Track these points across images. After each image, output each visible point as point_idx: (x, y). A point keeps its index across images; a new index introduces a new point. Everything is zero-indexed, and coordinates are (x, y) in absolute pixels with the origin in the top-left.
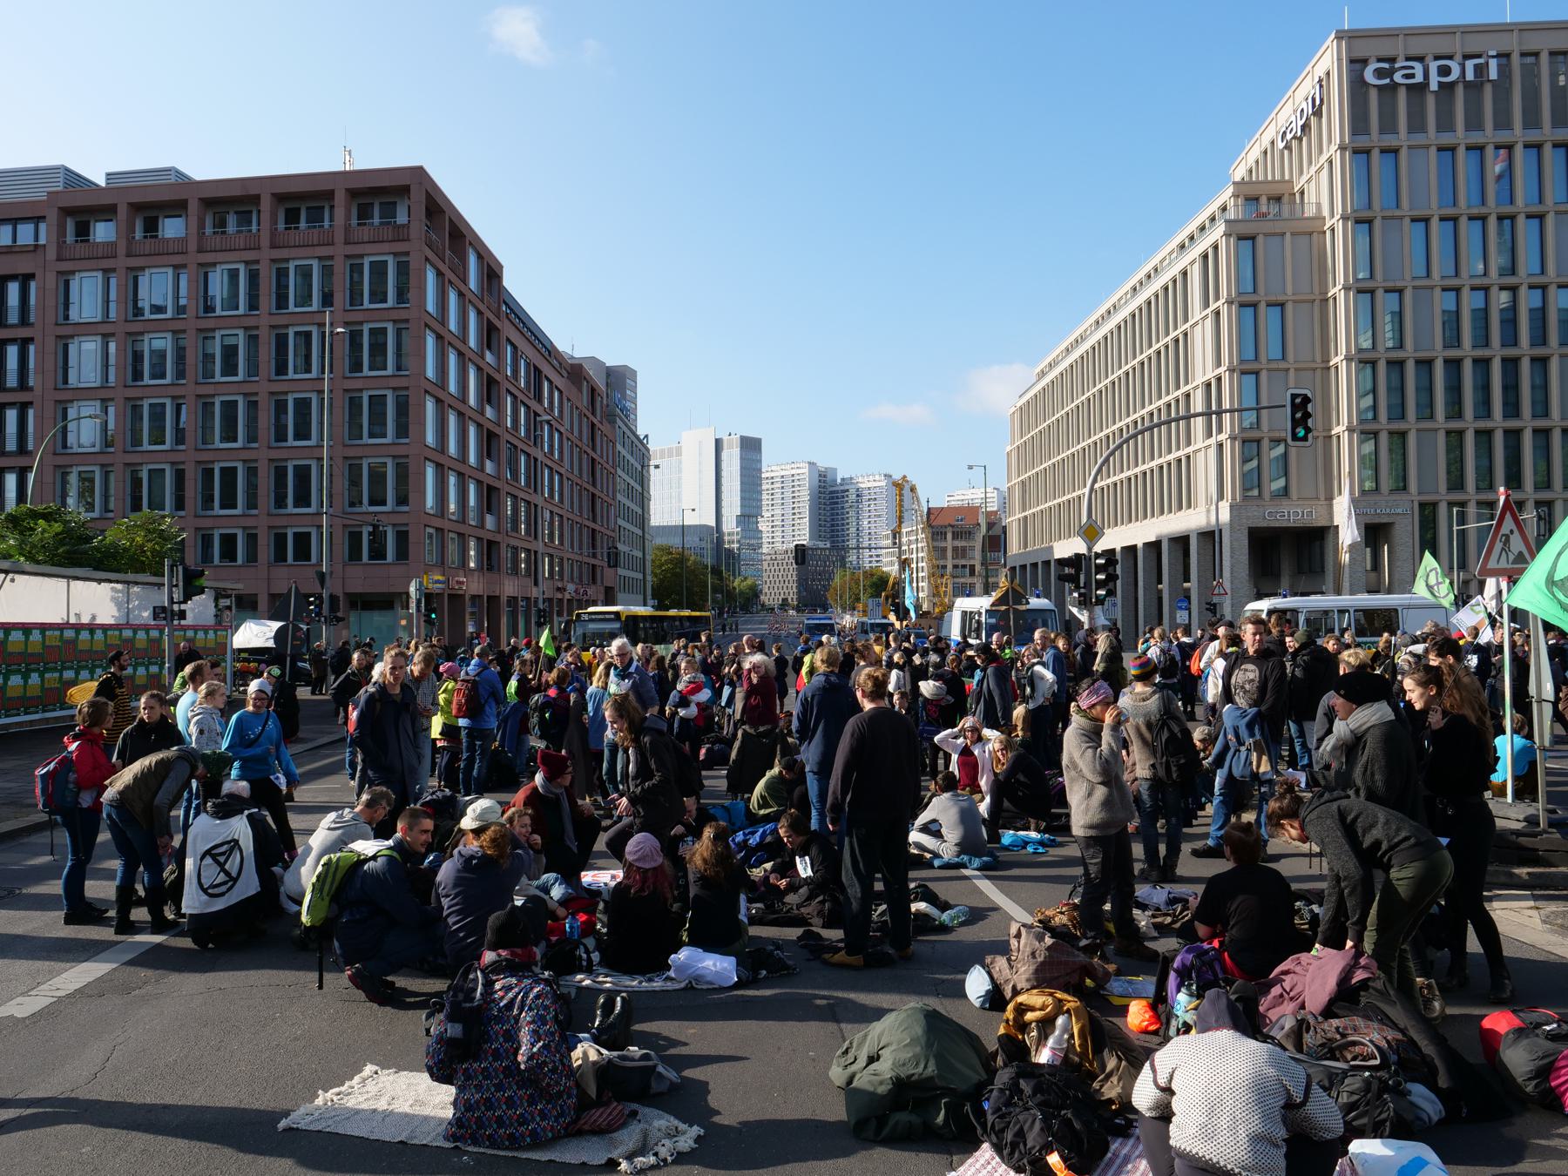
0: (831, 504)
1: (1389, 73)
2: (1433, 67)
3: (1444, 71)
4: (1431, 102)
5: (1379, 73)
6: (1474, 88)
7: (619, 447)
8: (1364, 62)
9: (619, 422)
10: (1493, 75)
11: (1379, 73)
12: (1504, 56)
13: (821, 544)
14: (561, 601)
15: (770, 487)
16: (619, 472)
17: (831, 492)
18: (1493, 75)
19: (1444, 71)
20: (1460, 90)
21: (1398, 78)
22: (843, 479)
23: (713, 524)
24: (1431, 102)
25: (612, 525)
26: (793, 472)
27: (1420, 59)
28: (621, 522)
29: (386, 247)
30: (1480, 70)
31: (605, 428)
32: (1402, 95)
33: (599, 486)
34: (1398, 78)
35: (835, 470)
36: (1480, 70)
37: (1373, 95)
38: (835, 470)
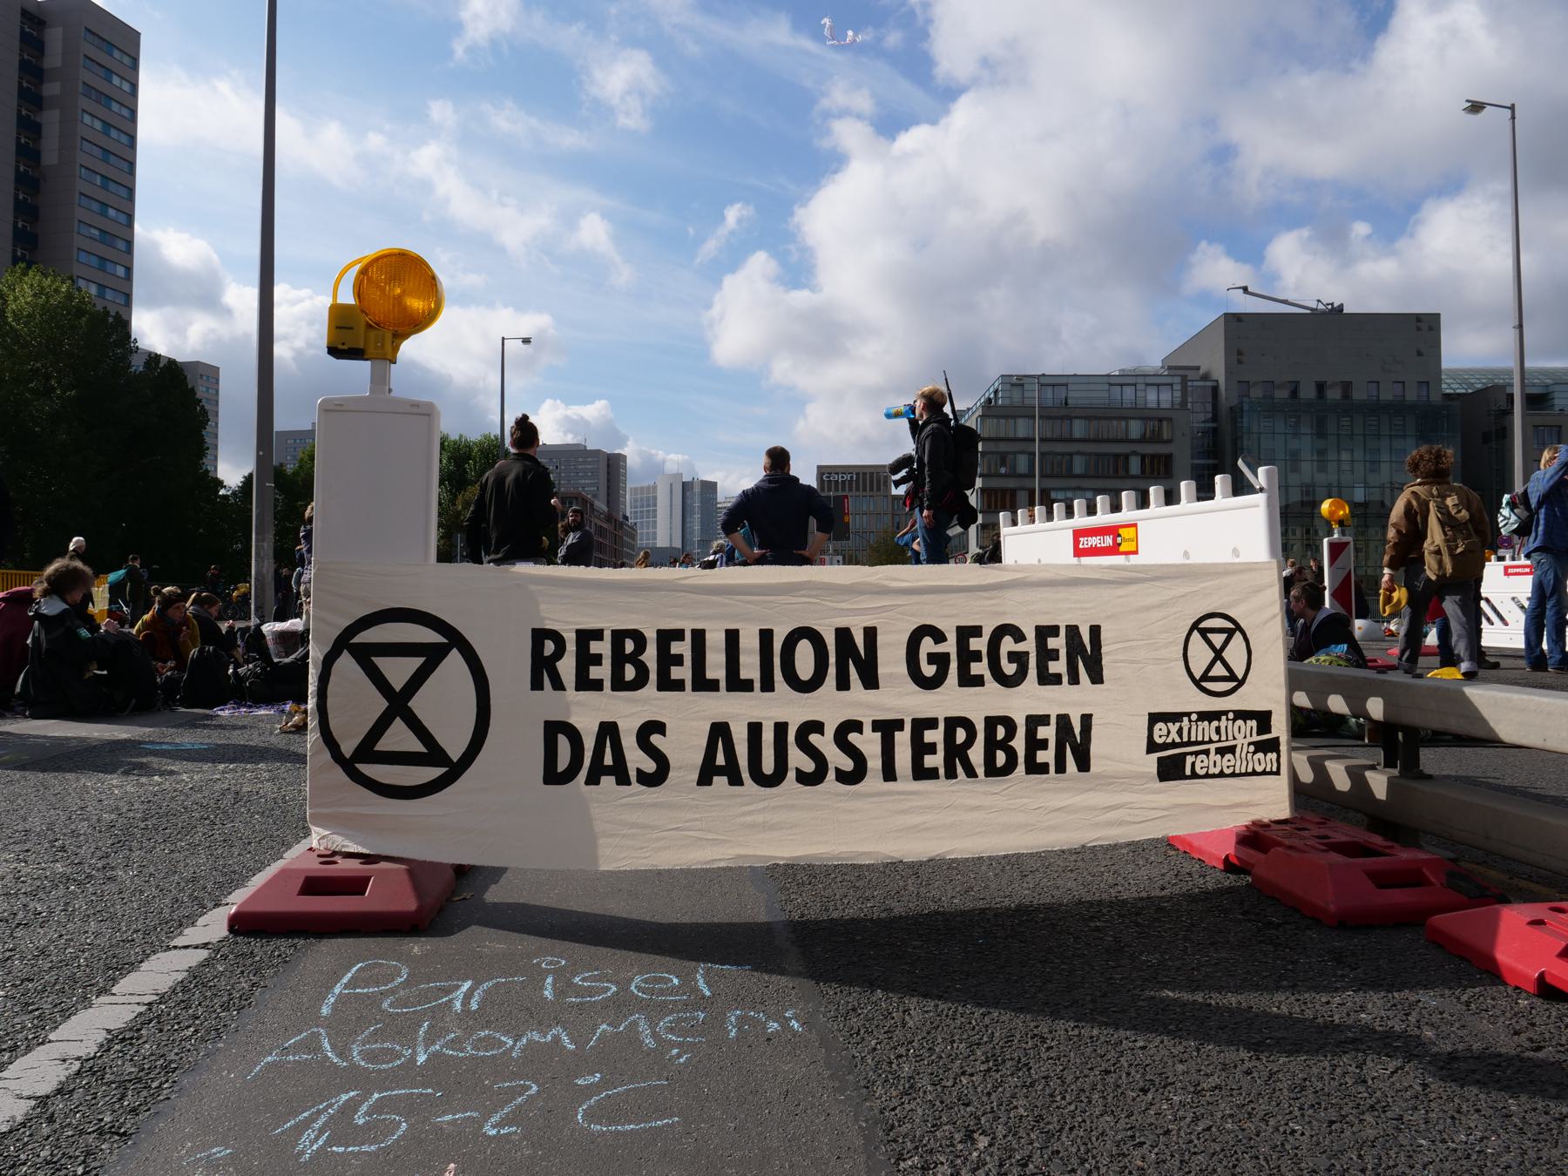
1: (829, 477)
2: (840, 476)
3: (843, 477)
4: (840, 485)
5: (827, 477)
6: (851, 481)
7: (625, 538)
8: (824, 474)
10: (854, 478)
11: (827, 477)
12: (857, 474)
16: (625, 549)
18: (854, 478)
19: (843, 477)
20: (847, 482)
21: (831, 478)
23: (680, 546)
24: (840, 485)
27: (837, 474)
30: (852, 477)
31: (620, 533)
32: (833, 483)
34: (831, 478)
36: (852, 477)
37: (826, 483)
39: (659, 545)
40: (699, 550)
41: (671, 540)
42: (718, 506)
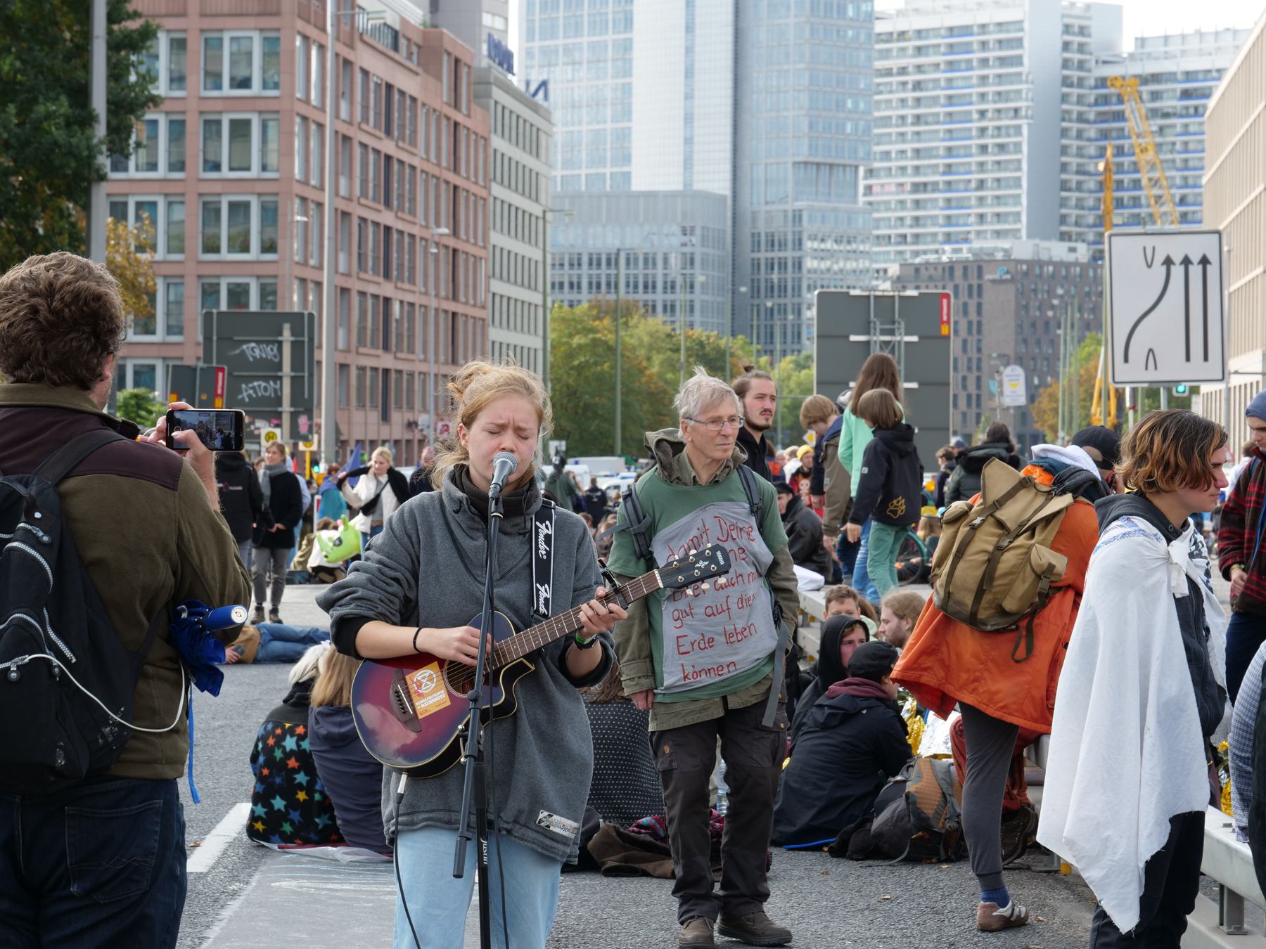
0: (1102, 118)
7: (497, 142)
9: (497, 94)
13: (1058, 251)
14: (409, 442)
15: (910, 62)
16: (497, 190)
17: (1102, 82)
22: (1142, 42)
23: (722, 186)
25: (481, 296)
26: (982, 18)
28: (498, 287)
29: (251, 22)
31: (471, 120)
33: (463, 236)
35: (1117, 10)
38: (1117, 10)
39: (638, 185)
40: (799, 205)
41: (688, 163)
42: (880, 27)
